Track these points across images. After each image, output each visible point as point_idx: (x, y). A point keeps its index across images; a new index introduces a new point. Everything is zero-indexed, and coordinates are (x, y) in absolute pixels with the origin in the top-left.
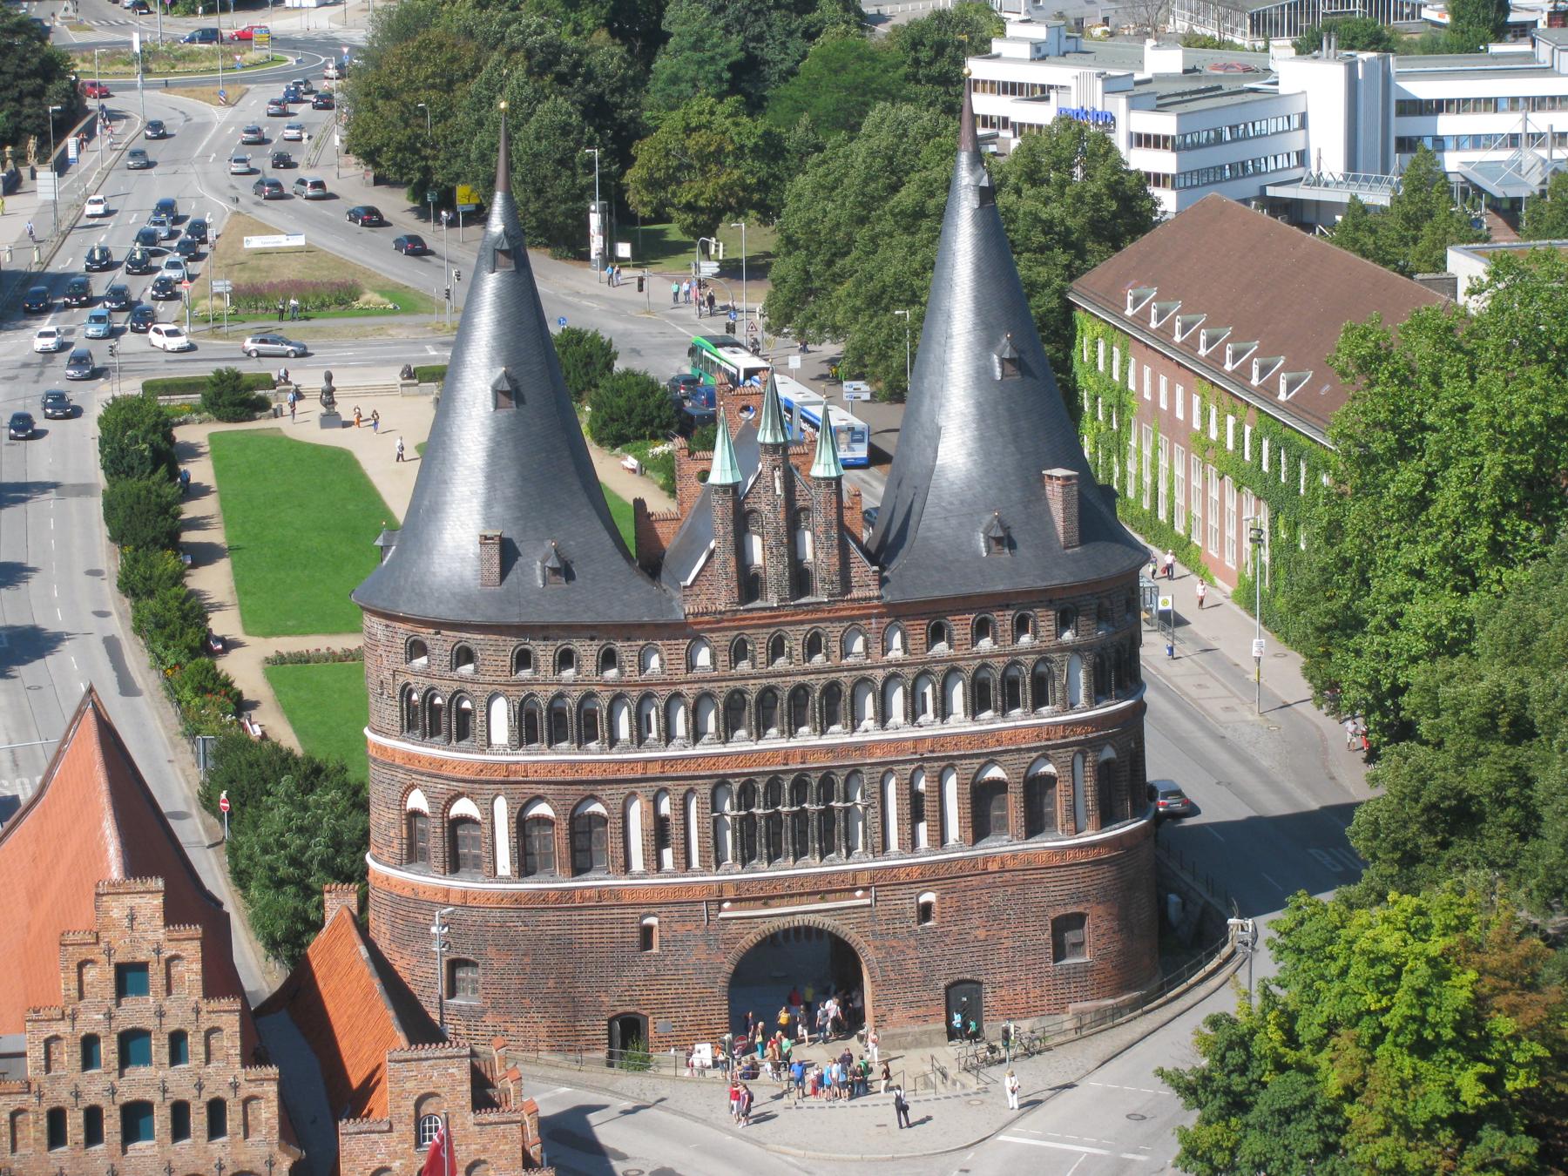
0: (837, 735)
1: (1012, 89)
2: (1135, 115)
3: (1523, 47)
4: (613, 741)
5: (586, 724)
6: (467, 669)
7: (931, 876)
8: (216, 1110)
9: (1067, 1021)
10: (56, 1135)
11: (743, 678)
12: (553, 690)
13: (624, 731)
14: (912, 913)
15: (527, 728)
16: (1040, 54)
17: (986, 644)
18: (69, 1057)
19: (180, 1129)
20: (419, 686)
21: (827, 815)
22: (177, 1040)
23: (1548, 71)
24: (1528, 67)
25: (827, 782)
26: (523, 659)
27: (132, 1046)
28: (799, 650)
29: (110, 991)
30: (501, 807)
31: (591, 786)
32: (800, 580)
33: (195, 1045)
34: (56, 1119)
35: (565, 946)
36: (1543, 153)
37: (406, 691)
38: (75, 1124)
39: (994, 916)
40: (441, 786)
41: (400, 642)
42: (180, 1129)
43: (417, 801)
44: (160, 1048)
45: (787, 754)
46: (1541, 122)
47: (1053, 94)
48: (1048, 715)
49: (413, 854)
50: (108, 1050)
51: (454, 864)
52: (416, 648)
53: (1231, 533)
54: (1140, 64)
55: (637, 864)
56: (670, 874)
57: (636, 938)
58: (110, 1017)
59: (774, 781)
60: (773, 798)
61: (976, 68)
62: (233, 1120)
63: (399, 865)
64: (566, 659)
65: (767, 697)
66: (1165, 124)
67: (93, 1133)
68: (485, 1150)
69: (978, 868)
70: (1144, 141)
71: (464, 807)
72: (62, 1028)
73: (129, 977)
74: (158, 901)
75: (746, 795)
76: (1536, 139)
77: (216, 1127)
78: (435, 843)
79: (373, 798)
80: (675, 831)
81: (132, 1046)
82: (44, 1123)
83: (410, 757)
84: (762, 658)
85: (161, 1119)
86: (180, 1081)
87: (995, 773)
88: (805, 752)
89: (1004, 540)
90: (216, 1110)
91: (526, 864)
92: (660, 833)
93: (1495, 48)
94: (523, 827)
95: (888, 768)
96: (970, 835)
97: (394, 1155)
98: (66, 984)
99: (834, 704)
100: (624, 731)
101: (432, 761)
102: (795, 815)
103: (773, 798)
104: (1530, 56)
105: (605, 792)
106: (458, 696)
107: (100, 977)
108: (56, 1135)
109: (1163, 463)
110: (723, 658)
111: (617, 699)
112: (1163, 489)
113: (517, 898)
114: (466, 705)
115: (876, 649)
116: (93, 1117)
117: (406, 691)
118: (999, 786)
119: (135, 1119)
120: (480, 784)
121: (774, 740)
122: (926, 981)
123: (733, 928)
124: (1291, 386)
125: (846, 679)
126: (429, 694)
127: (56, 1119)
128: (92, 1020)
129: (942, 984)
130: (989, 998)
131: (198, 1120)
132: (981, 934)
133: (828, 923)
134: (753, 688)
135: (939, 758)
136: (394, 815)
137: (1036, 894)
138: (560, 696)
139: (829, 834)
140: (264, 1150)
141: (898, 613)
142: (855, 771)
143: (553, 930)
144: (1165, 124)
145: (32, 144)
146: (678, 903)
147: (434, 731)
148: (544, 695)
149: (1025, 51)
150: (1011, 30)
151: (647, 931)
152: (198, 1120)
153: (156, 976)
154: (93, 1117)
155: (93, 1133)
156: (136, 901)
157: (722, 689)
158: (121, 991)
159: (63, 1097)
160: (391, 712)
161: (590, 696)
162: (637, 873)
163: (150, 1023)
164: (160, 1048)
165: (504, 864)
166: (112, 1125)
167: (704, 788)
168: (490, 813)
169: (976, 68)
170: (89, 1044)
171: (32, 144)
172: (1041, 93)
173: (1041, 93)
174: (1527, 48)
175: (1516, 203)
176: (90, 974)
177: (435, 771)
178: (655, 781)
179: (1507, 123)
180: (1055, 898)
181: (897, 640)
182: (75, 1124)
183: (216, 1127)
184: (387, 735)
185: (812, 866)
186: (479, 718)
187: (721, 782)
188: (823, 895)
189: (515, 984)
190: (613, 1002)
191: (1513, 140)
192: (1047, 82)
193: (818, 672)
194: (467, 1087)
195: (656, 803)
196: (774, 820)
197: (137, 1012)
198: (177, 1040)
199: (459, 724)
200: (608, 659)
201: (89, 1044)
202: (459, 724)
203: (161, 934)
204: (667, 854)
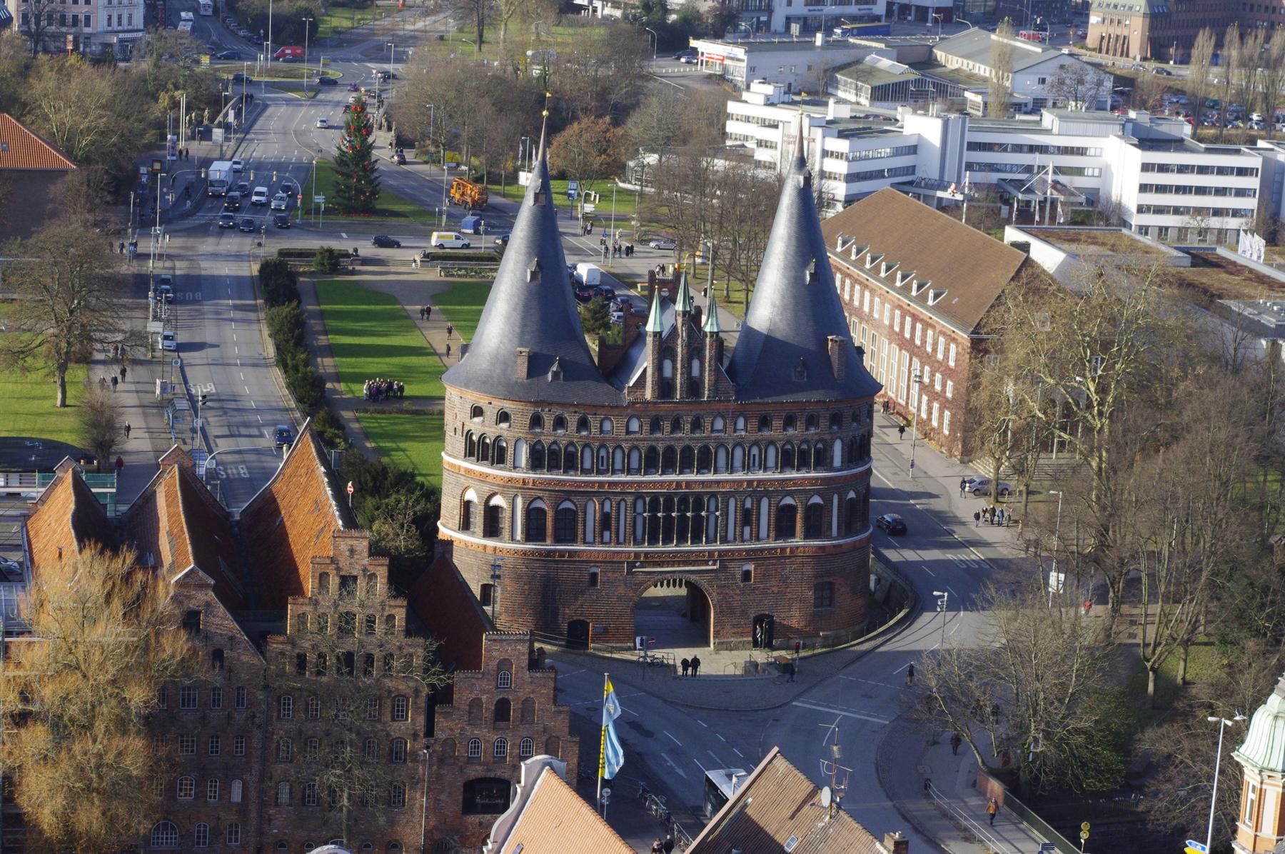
2: (828, 140)
5: (571, 463)
6: (504, 425)
7: (751, 555)
11: (657, 440)
12: (552, 439)
14: (739, 576)
15: (536, 461)
16: (769, 103)
21: (698, 519)
31: (568, 495)
32: (694, 387)
43: (471, 495)
47: (781, 125)
49: (465, 525)
55: (590, 537)
57: (587, 578)
58: (336, 606)
59: (669, 498)
60: (669, 508)
61: (732, 107)
64: (560, 423)
65: (670, 450)
66: (843, 145)
68: (533, 692)
69: (781, 556)
73: (347, 581)
74: (366, 543)
75: (654, 506)
78: (478, 519)
79: (444, 491)
87: (788, 501)
96: (772, 534)
97: (483, 691)
102: (676, 518)
103: (669, 508)
106: (498, 438)
110: (646, 428)
111: (586, 446)
115: (730, 429)
117: (469, 435)
118: (792, 509)
122: (744, 613)
124: (936, 296)
129: (752, 616)
132: (775, 589)
133: (693, 578)
135: (758, 491)
138: (555, 442)
142: (713, 495)
146: (611, 562)
147: (485, 458)
148: (546, 440)
149: (761, 100)
151: (594, 575)
156: (354, 542)
157: (644, 446)
161: (571, 444)
167: (630, 499)
169: (732, 107)
174: (1037, 118)
177: (483, 478)
178: (602, 493)
184: (455, 457)
186: (510, 451)
188: (686, 563)
192: (777, 118)
193: (698, 439)
194: (527, 656)
195: (602, 505)
196: (668, 519)
200: (583, 424)
203: (366, 561)
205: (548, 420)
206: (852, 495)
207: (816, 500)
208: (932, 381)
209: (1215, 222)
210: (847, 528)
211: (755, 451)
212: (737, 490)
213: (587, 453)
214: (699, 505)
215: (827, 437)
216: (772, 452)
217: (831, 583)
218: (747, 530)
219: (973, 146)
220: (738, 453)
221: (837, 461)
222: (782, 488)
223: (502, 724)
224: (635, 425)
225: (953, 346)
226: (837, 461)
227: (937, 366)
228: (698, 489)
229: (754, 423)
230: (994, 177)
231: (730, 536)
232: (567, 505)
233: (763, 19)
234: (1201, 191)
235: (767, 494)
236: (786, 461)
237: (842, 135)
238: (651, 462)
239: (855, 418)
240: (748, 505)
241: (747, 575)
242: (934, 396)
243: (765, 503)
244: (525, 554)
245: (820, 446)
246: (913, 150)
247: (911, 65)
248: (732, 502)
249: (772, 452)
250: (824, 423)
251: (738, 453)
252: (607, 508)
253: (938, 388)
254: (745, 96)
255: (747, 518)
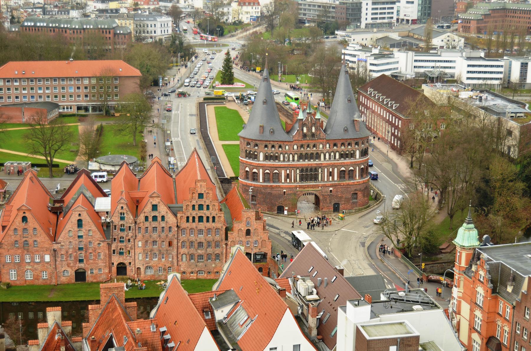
0: (317, 162)
1: (350, 55)
3: (436, 52)
4: (280, 161)
5: (277, 158)
6: (256, 148)
7: (331, 186)
8: (214, 218)
9: (354, 211)
10: (188, 221)
13: (282, 159)
15: (267, 158)
17: (343, 147)
18: (191, 208)
19: (208, 221)
20: (249, 150)
22: (208, 206)
23: (440, 56)
24: (436, 55)
25: (316, 169)
26: (266, 146)
27: (201, 207)
28: (312, 147)
29: (197, 197)
30: (261, 171)
31: (276, 168)
32: (313, 135)
33: (211, 207)
34: (188, 218)
35: (270, 194)
36: (438, 69)
37: (246, 151)
38: (191, 219)
39: (342, 192)
40: (252, 167)
41: (246, 143)
42: (208, 221)
43: (247, 169)
44: (205, 208)
45: (309, 164)
46: (438, 64)
48: (352, 160)
49: (247, 178)
50: (197, 207)
51: (254, 180)
52: (248, 144)
53: (384, 131)
54: (371, 52)
55: (283, 181)
56: (288, 183)
58: (197, 202)
62: (216, 220)
63: (244, 179)
67: (194, 221)
69: (340, 185)
70: (371, 64)
71: (255, 170)
72: (189, 203)
75: (302, 171)
76: (438, 67)
77: (214, 221)
80: (290, 176)
81: (201, 207)
82: (186, 219)
83: (246, 162)
84: (306, 148)
85: (205, 219)
86: (208, 213)
87: (343, 169)
88: (312, 164)
89: (346, 130)
90: (214, 218)
91: (264, 181)
92: (288, 176)
93: (431, 52)
94: (264, 174)
95: (326, 167)
98: (190, 196)
99: (318, 156)
100: (282, 159)
101: (250, 163)
104: (437, 53)
105: (279, 169)
106: (255, 152)
107: (196, 196)
108: (188, 221)
109: (373, 119)
112: (373, 123)
113: (263, 186)
114: (256, 153)
116: (194, 218)
117: (246, 151)
119: (201, 219)
120: (258, 167)
121: (306, 162)
123: (299, 192)
124: (395, 106)
125: (319, 152)
126: (250, 151)
127: (188, 218)
128: (194, 202)
130: (341, 206)
131: (211, 219)
133: (314, 192)
134: (304, 153)
135: (333, 166)
136: (243, 171)
137: (349, 189)
139: (316, 178)
140: (221, 225)
141: (328, 141)
143: (269, 191)
144: (375, 62)
145: (187, 58)
150: (350, 45)
152: (211, 219)
153: (205, 196)
154: (194, 218)
155: (194, 221)
158: (199, 198)
159: (189, 215)
160: (244, 154)
162: (283, 183)
163: (203, 203)
164: (205, 208)
165: (261, 180)
166: (197, 219)
168: (259, 171)
170: (194, 206)
171: (187, 58)
172: (354, 56)
173: (354, 56)
174: (436, 52)
175: (433, 78)
176: (194, 195)
179: (433, 64)
180: (353, 189)
181: (328, 146)
182: (191, 219)
183: (214, 221)
185: (312, 183)
187: (298, 168)
189: (262, 200)
190: (278, 204)
191: (433, 67)
194: (254, 216)
197: (201, 202)
198: (208, 206)
199: (256, 157)
201: (194, 206)
202: (256, 157)
204: (288, 180)
205: (270, 146)
206: (362, 166)
207: (351, 168)
208: (395, 132)
209: (489, 82)
210: (361, 176)
211: (332, 154)
212: (328, 166)
213: (282, 156)
214: (316, 170)
215: (354, 149)
216: (337, 154)
217: (356, 193)
218: (331, 178)
219: (415, 61)
220: (327, 155)
221: (358, 157)
222: (343, 165)
223: (248, 237)
224: (295, 147)
225: (400, 121)
226: (358, 157)
227: (396, 127)
228: (315, 165)
229: (332, 145)
230: (422, 70)
231: (326, 180)
232: (276, 171)
233: (359, 24)
234: (485, 72)
235: (336, 166)
236: (341, 156)
237: (375, 59)
238: (301, 157)
239: (363, 143)
240: (331, 170)
241: (331, 191)
242: (396, 137)
243: (336, 170)
244: (243, 185)
245: (352, 152)
246: (398, 62)
247: (402, 37)
248: (326, 170)
249: (337, 154)
250: (353, 145)
251: (327, 155)
252: (288, 172)
253: (396, 134)
254: (347, 48)
255: (331, 174)
